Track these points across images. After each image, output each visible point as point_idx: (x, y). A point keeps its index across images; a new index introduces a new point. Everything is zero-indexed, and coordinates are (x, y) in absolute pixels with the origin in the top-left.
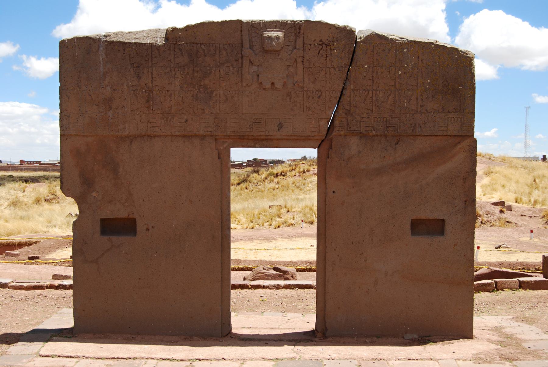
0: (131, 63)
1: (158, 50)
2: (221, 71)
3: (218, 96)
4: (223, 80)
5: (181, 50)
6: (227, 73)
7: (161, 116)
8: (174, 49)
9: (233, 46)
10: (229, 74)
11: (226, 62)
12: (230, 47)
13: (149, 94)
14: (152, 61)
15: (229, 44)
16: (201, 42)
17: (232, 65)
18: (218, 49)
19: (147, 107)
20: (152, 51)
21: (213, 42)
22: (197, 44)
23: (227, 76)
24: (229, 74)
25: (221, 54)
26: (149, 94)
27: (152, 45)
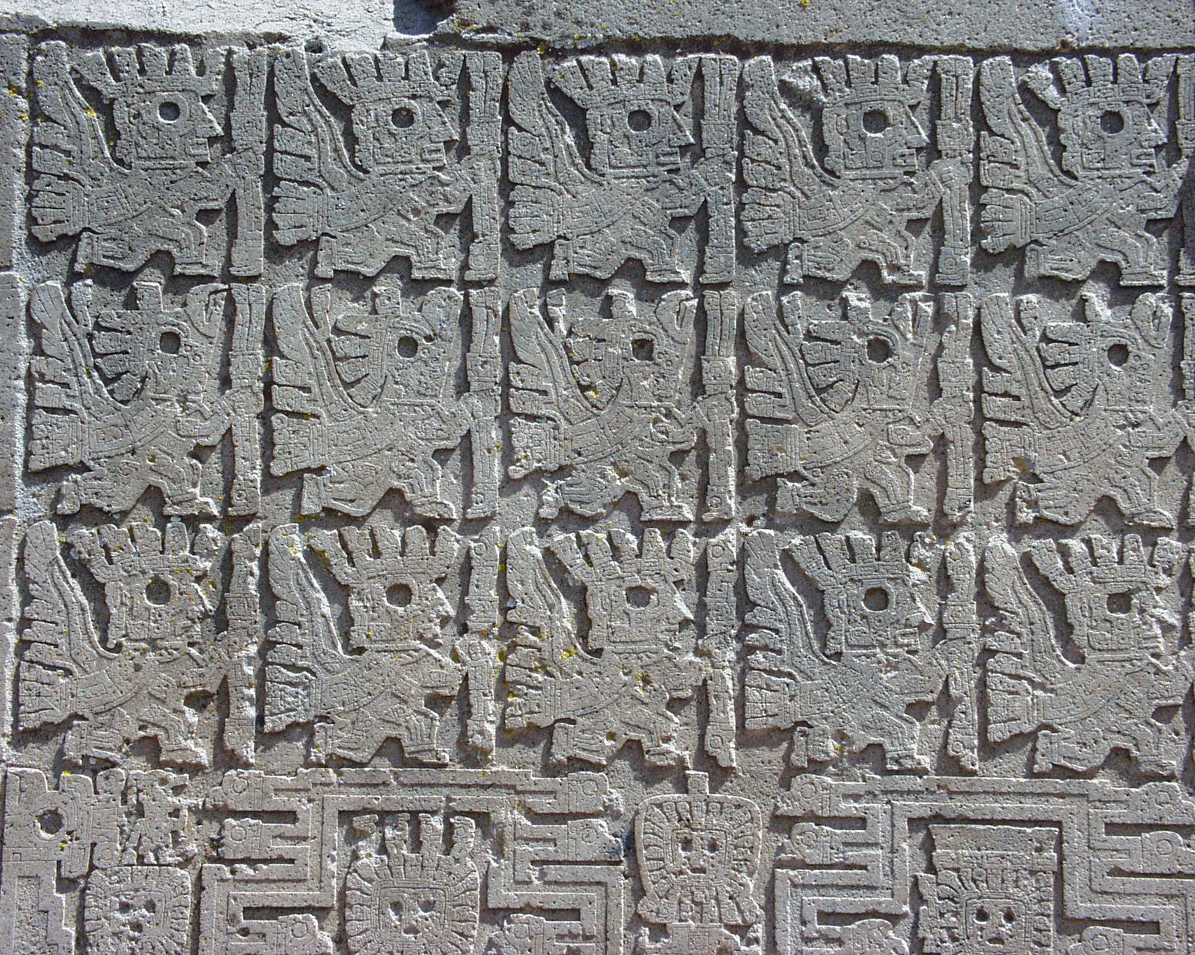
0: (45, 233)
1: (342, 110)
2: (989, 332)
3: (966, 583)
4: (1018, 424)
5: (575, 114)
6: (1051, 351)
7: (354, 798)
8: (505, 100)
9: (1116, 74)
10: (1076, 354)
11: (1040, 237)
12: (1089, 82)
13: (227, 563)
14: (271, 225)
15: (1079, 53)
16: (787, 36)
17: (1108, 272)
18: (966, 103)
19: (198, 701)
20: (274, 118)
21: (913, 36)
22: (743, 49)
23: (1061, 377)
24: (1076, 354)
25: (991, 157)
26: (227, 563)
27: (273, 57)
